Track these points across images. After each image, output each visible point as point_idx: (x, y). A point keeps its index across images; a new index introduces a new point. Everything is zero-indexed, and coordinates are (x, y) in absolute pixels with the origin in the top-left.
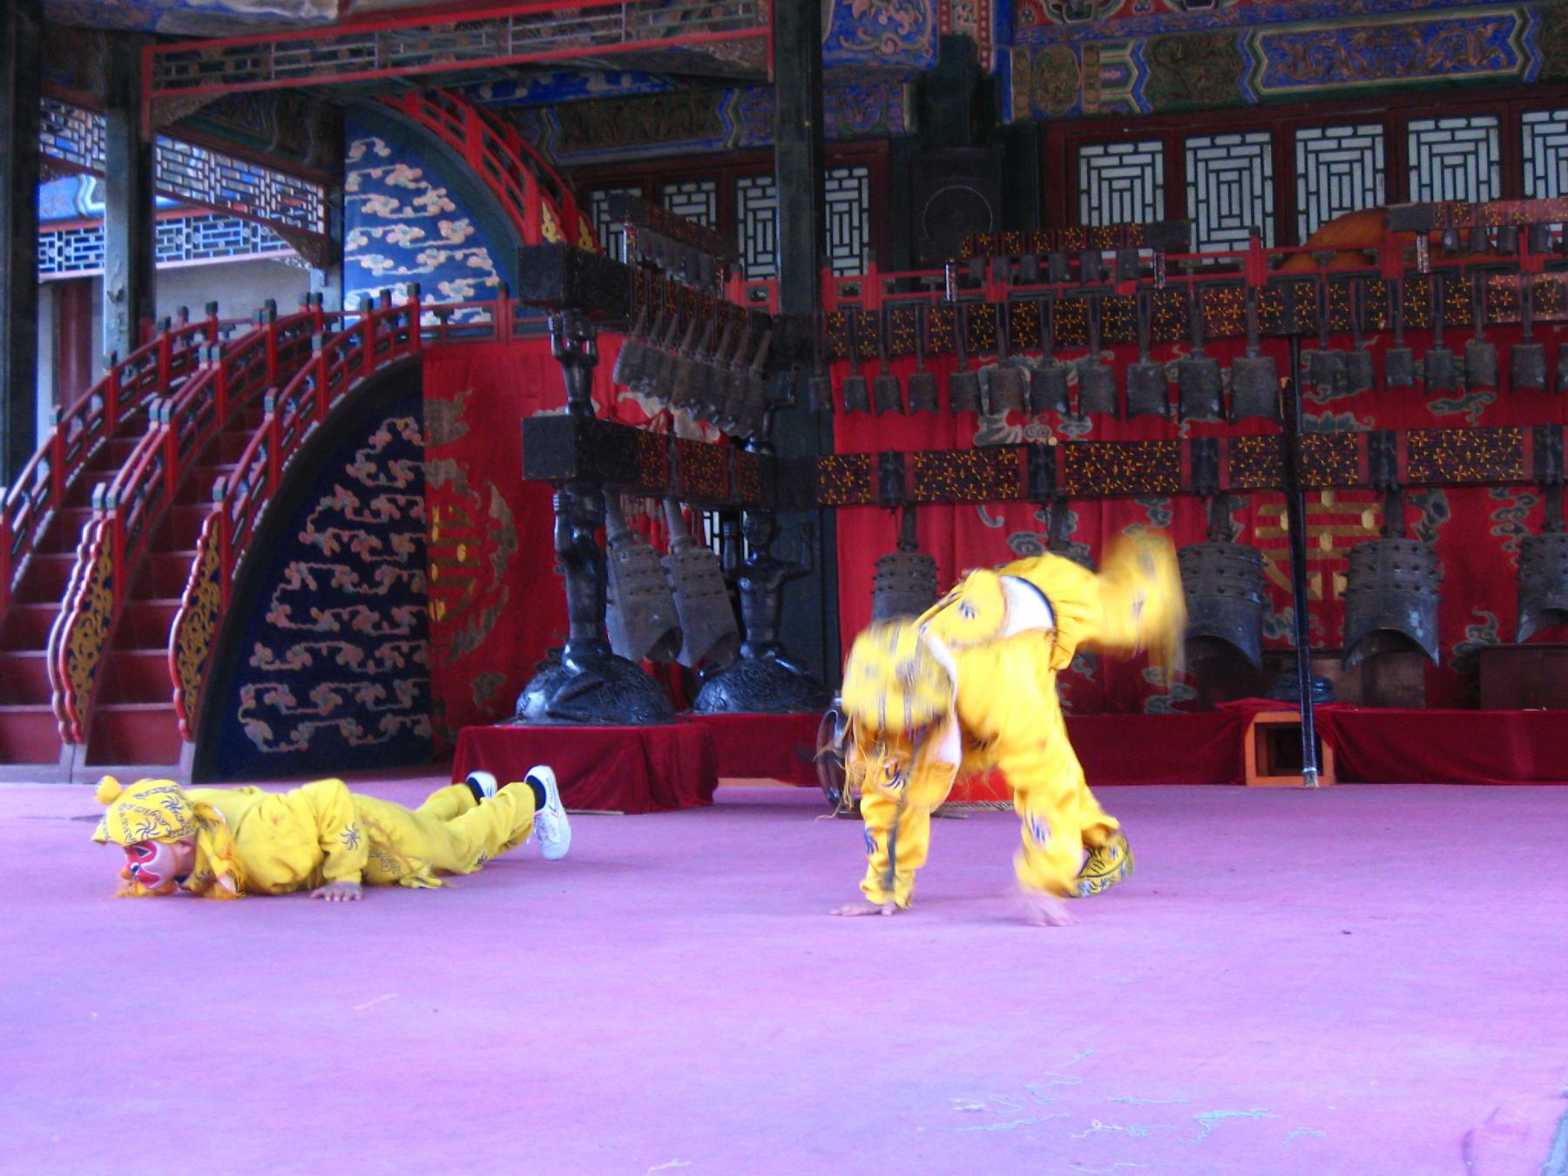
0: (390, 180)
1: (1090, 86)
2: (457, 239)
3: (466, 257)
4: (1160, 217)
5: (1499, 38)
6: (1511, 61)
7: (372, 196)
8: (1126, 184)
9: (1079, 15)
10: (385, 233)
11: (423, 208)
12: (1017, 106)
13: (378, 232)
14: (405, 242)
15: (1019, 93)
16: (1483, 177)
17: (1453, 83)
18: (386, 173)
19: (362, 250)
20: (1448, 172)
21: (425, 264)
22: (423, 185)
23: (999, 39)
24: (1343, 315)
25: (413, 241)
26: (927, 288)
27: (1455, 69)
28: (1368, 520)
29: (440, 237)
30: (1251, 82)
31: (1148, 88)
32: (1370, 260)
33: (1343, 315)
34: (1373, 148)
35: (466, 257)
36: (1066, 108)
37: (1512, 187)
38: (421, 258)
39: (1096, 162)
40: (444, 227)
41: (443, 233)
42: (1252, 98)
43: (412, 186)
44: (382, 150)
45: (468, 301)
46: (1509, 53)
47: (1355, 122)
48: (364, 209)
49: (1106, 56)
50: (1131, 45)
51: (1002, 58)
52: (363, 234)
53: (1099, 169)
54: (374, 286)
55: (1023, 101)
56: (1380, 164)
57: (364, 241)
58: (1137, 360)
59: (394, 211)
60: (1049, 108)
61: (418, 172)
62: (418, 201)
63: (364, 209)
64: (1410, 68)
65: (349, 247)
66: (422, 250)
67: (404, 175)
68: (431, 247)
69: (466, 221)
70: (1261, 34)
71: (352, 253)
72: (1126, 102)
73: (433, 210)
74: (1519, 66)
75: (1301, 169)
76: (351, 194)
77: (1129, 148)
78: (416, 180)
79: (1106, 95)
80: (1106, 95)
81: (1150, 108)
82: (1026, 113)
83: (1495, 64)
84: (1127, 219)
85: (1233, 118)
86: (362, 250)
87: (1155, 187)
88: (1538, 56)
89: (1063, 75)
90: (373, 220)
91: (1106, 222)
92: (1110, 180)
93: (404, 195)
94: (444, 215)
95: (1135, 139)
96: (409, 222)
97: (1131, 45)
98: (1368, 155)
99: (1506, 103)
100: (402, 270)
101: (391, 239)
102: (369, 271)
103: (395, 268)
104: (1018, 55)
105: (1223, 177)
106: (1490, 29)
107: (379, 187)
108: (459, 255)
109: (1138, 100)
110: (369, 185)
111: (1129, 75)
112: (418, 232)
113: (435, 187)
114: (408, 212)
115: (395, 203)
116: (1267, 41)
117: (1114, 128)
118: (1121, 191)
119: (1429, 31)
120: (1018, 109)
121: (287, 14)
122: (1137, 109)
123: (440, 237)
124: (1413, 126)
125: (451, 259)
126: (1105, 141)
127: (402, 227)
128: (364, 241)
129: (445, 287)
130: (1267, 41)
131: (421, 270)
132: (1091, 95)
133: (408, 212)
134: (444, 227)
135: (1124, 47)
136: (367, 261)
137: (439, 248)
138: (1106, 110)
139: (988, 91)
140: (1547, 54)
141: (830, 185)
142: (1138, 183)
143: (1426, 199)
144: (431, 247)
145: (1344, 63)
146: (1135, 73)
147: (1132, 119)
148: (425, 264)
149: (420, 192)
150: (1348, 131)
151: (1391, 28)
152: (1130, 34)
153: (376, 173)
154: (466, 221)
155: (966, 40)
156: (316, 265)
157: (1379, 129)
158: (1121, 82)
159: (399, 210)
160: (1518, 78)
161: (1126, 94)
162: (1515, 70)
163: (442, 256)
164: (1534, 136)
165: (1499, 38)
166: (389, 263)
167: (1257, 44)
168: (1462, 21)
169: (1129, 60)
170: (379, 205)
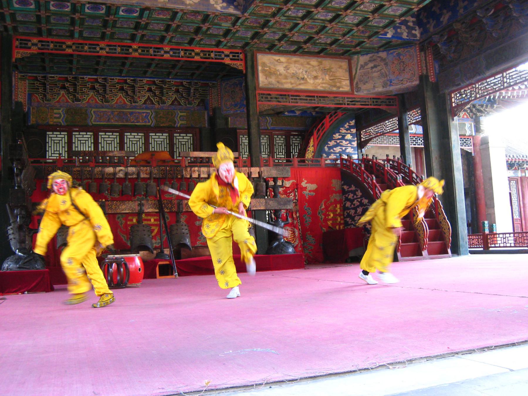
1: (51, 118)
4: (93, 149)
5: (146, 117)
6: (149, 122)
8: (58, 141)
9: (48, 101)
12: (32, 120)
15: (33, 118)
16: (90, 146)
17: (136, 125)
20: (55, 144)
23: (28, 104)
24: (171, 174)
26: (41, 163)
27: (137, 122)
28: (135, 221)
30: (91, 121)
31: (66, 119)
32: (149, 163)
33: (171, 174)
34: (117, 138)
36: (45, 122)
37: (122, 148)
39: (50, 136)
42: (90, 124)
46: (148, 120)
47: (113, 132)
49: (55, 111)
50: (62, 109)
51: (29, 109)
53: (51, 137)
55: (34, 119)
56: (118, 142)
58: (125, 182)
60: (40, 122)
64: (127, 121)
70: (93, 110)
72: (60, 122)
74: (151, 122)
75: (100, 141)
77: (59, 133)
79: (55, 120)
80: (55, 120)
81: (66, 124)
82: (35, 122)
83: (145, 122)
84: (85, 150)
85: (85, 128)
87: (65, 143)
88: (154, 122)
89: (44, 114)
91: (131, 150)
92: (54, 140)
95: (60, 131)
97: (62, 109)
98: (115, 139)
99: (146, 130)
104: (33, 108)
105: (82, 142)
106: (145, 114)
109: (63, 122)
111: (61, 116)
116: (94, 112)
117: (55, 128)
118: (57, 143)
119: (131, 113)
120: (33, 121)
122: (63, 124)
124: (126, 134)
126: (53, 131)
130: (94, 112)
132: (51, 120)
135: (60, 109)
138: (55, 124)
139: (26, 116)
140: (157, 121)
141: (261, 138)
142: (61, 142)
143: (128, 150)
145: (112, 118)
146: (63, 116)
147: (61, 126)
150: (111, 134)
151: (123, 112)
152: (61, 106)
155: (21, 103)
157: (118, 134)
158: (59, 118)
160: (150, 126)
161: (60, 120)
162: (150, 124)
164: (49, 137)
165: (146, 117)
167: (92, 112)
168: (139, 112)
169: (61, 113)
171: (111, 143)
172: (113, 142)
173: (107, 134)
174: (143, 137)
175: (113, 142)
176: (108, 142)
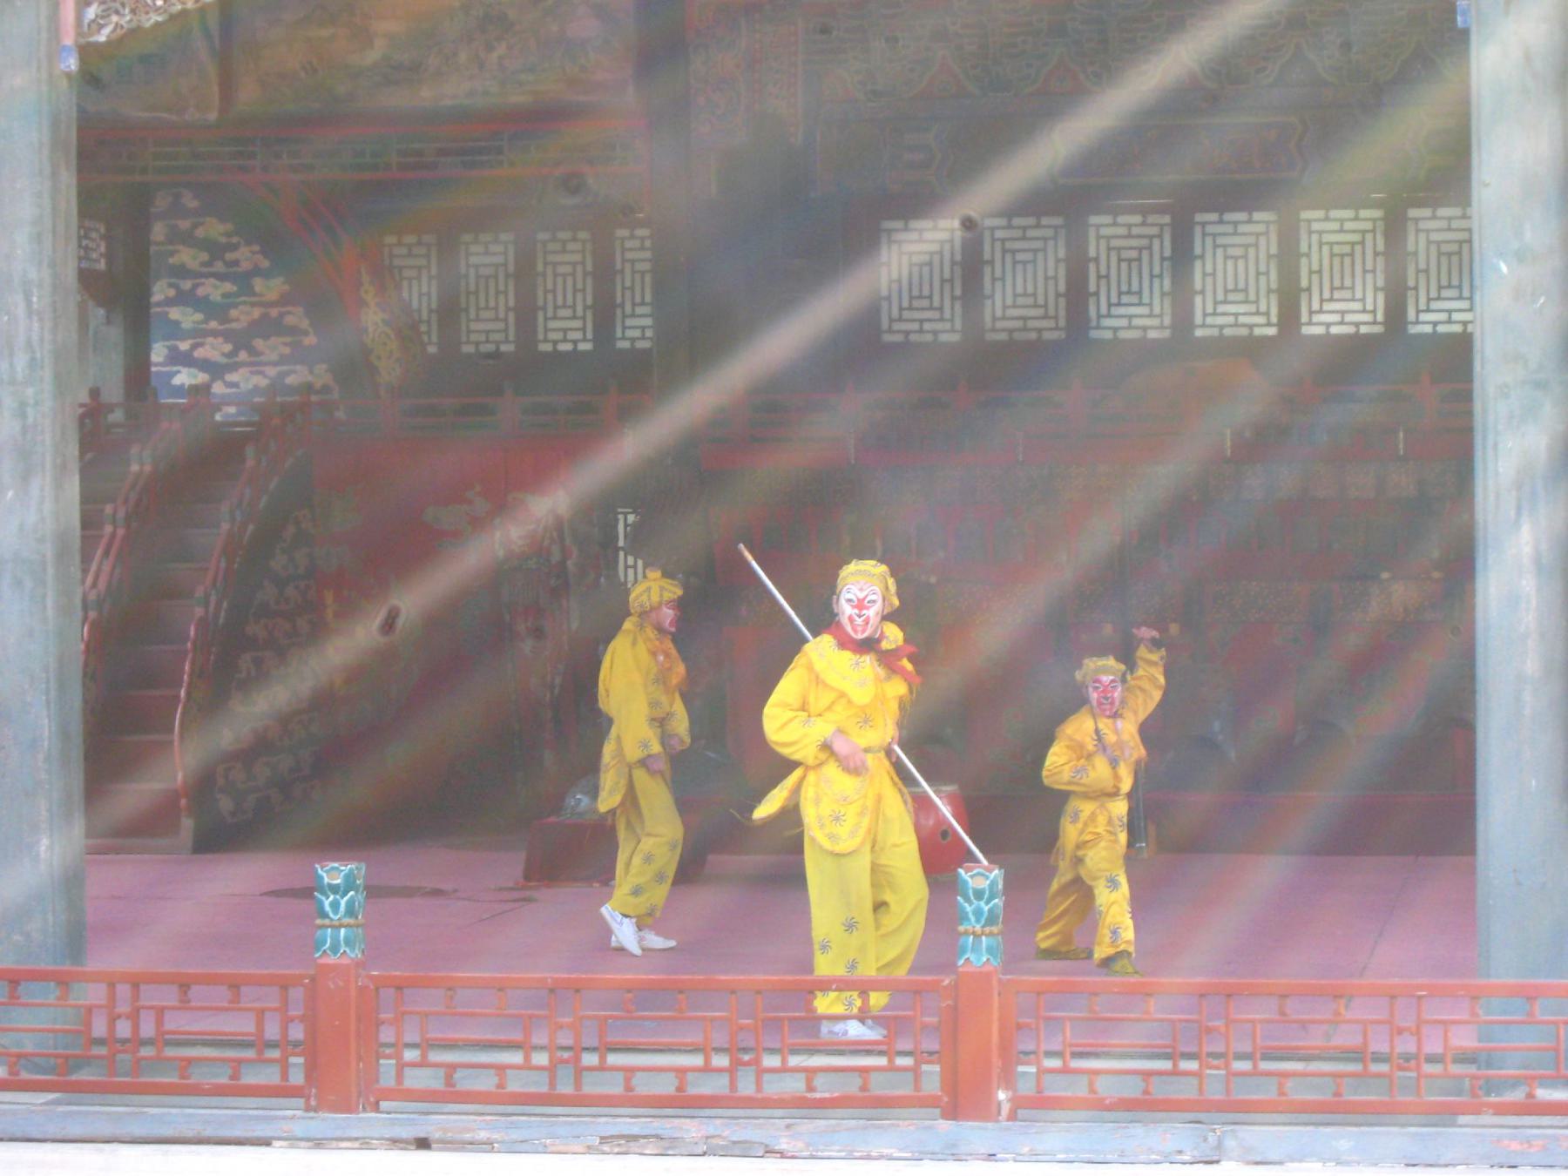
0: (200, 233)
2: (272, 296)
3: (281, 315)
7: (181, 247)
10: (195, 286)
11: (236, 263)
13: (187, 285)
14: (216, 296)
18: (195, 226)
19: (169, 302)
21: (237, 320)
22: (235, 240)
25: (224, 296)
29: (255, 294)
34: (1160, 236)
35: (281, 315)
38: (234, 313)
40: (258, 284)
41: (257, 289)
43: (223, 240)
44: (190, 202)
45: (283, 360)
48: (171, 261)
52: (171, 285)
54: (183, 339)
56: (1167, 253)
57: (172, 293)
59: (203, 264)
61: (229, 227)
62: (229, 256)
63: (171, 261)
65: (157, 296)
66: (235, 306)
67: (215, 229)
68: (245, 303)
69: (281, 279)
71: (159, 304)
73: (245, 266)
76: (158, 244)
78: (228, 235)
86: (169, 302)
90: (181, 272)
93: (216, 250)
94: (256, 271)
96: (221, 277)
98: (1156, 242)
100: (213, 324)
101: (200, 292)
102: (177, 323)
103: (206, 321)
107: (188, 239)
108: (274, 312)
110: (176, 237)
112: (229, 287)
113: (248, 243)
114: (219, 267)
115: (205, 256)
121: (174, 118)
123: (255, 294)
125: (265, 316)
127: (212, 280)
128: (172, 293)
129: (259, 343)
131: (234, 325)
133: (219, 267)
134: (258, 284)
136: (175, 314)
137: (253, 305)
144: (245, 303)
148: (237, 320)
149: (235, 247)
150: (1137, 219)
153: (184, 224)
154: (281, 279)
156: (100, 304)
157: (1167, 219)
159: (209, 264)
163: (257, 313)
166: (199, 316)
170: (187, 257)
171: (1139, 260)
172: (1145, 254)
173: (1120, 219)
174: (1273, 228)
175: (1145, 254)
176: (1125, 254)
